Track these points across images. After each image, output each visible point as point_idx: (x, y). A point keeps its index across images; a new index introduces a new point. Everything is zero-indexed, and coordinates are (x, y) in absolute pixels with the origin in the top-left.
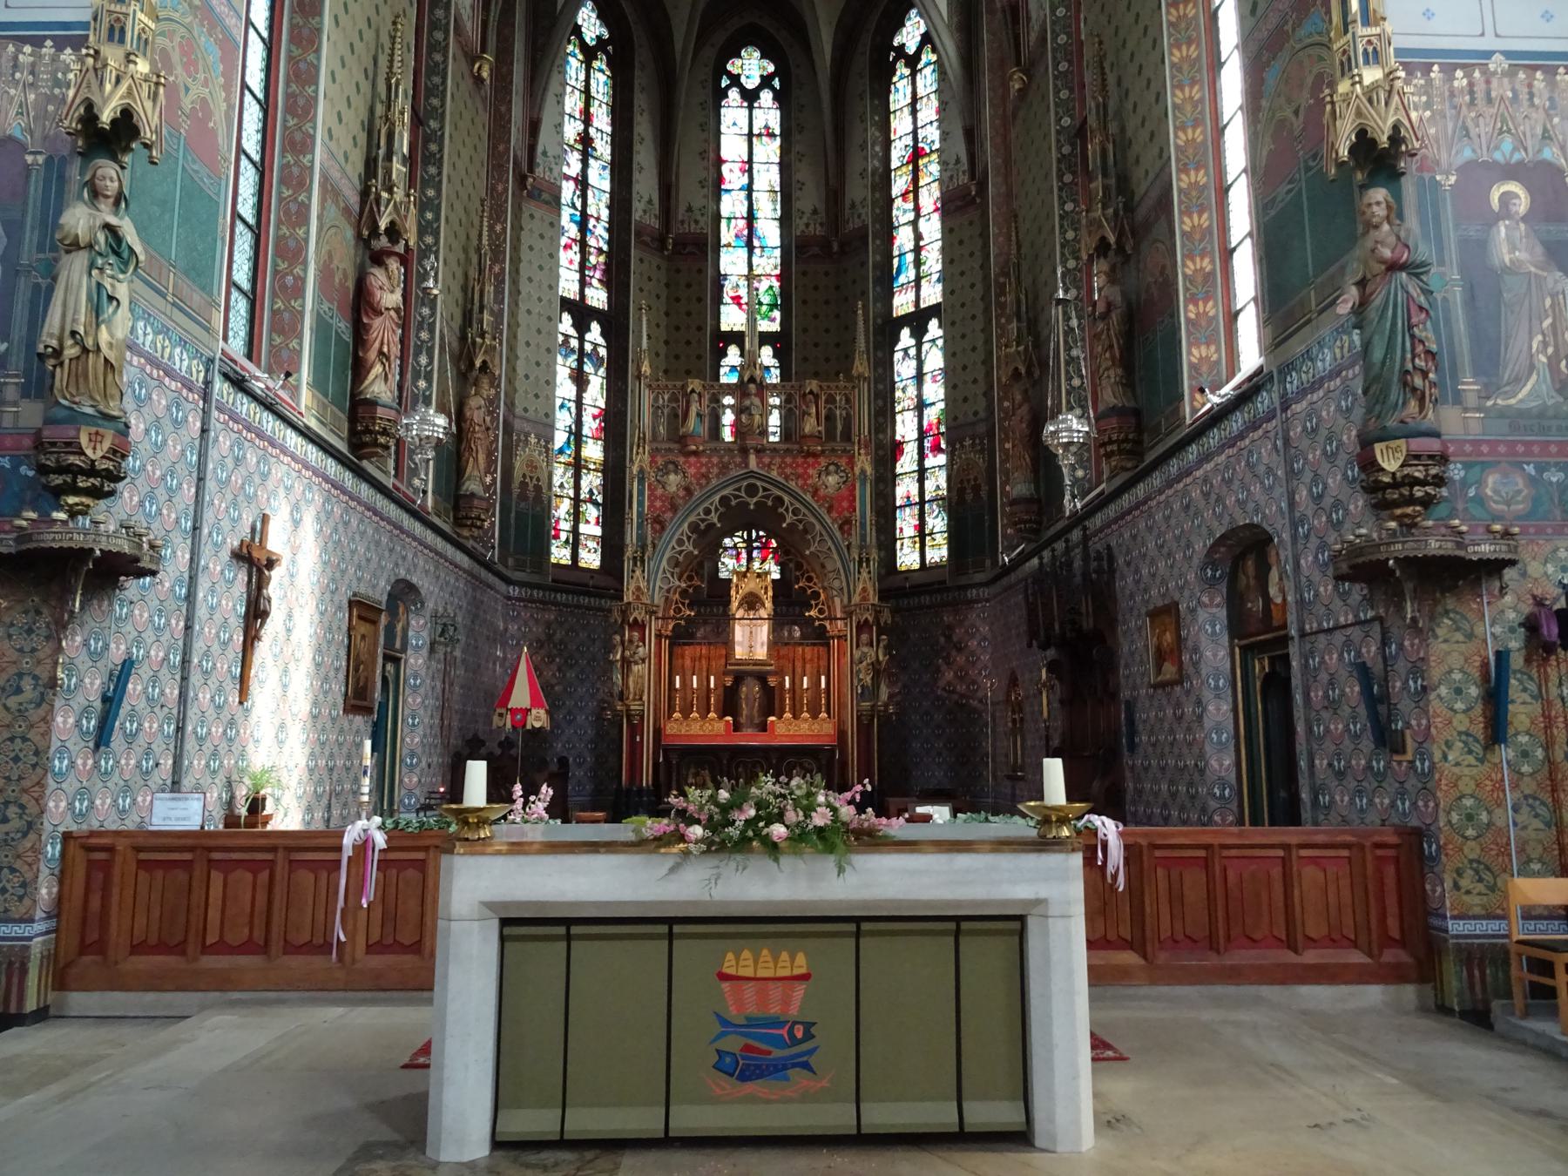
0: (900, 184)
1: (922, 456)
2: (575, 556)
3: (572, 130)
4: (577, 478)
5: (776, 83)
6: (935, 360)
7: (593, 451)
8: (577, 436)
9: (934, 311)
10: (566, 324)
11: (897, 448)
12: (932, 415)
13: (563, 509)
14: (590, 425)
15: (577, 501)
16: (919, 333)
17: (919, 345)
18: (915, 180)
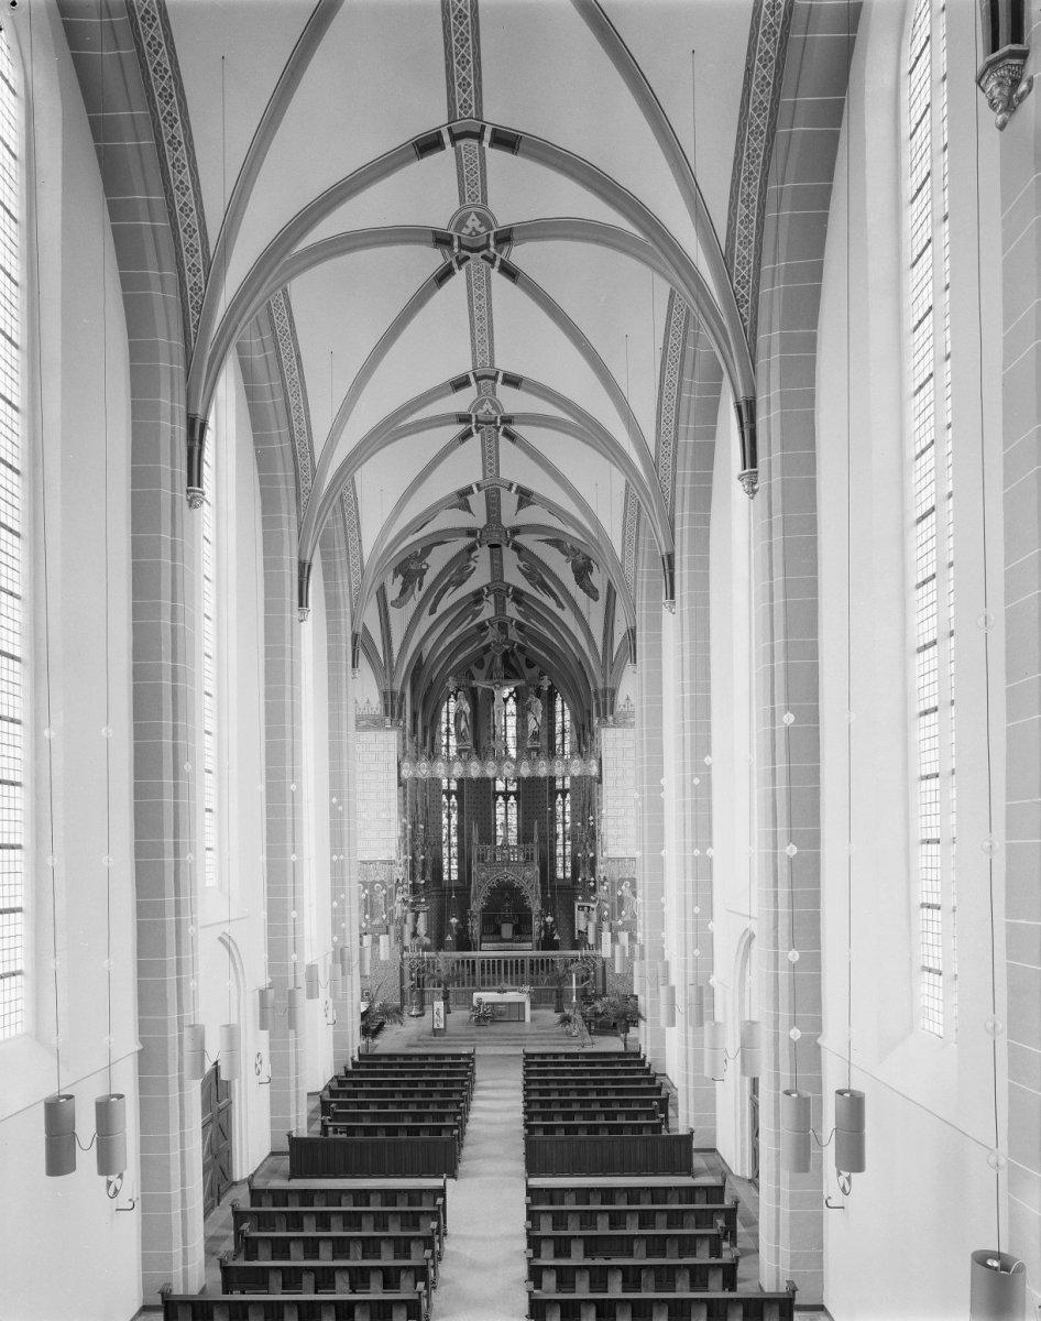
0: (558, 741)
1: (564, 841)
2: (450, 877)
3: (444, 727)
4: (449, 850)
5: (514, 695)
6: (568, 808)
7: (454, 840)
8: (449, 836)
9: (567, 791)
10: (444, 798)
11: (557, 836)
12: (568, 826)
13: (445, 861)
14: (453, 831)
15: (450, 859)
16: (564, 797)
17: (564, 801)
18: (563, 740)
